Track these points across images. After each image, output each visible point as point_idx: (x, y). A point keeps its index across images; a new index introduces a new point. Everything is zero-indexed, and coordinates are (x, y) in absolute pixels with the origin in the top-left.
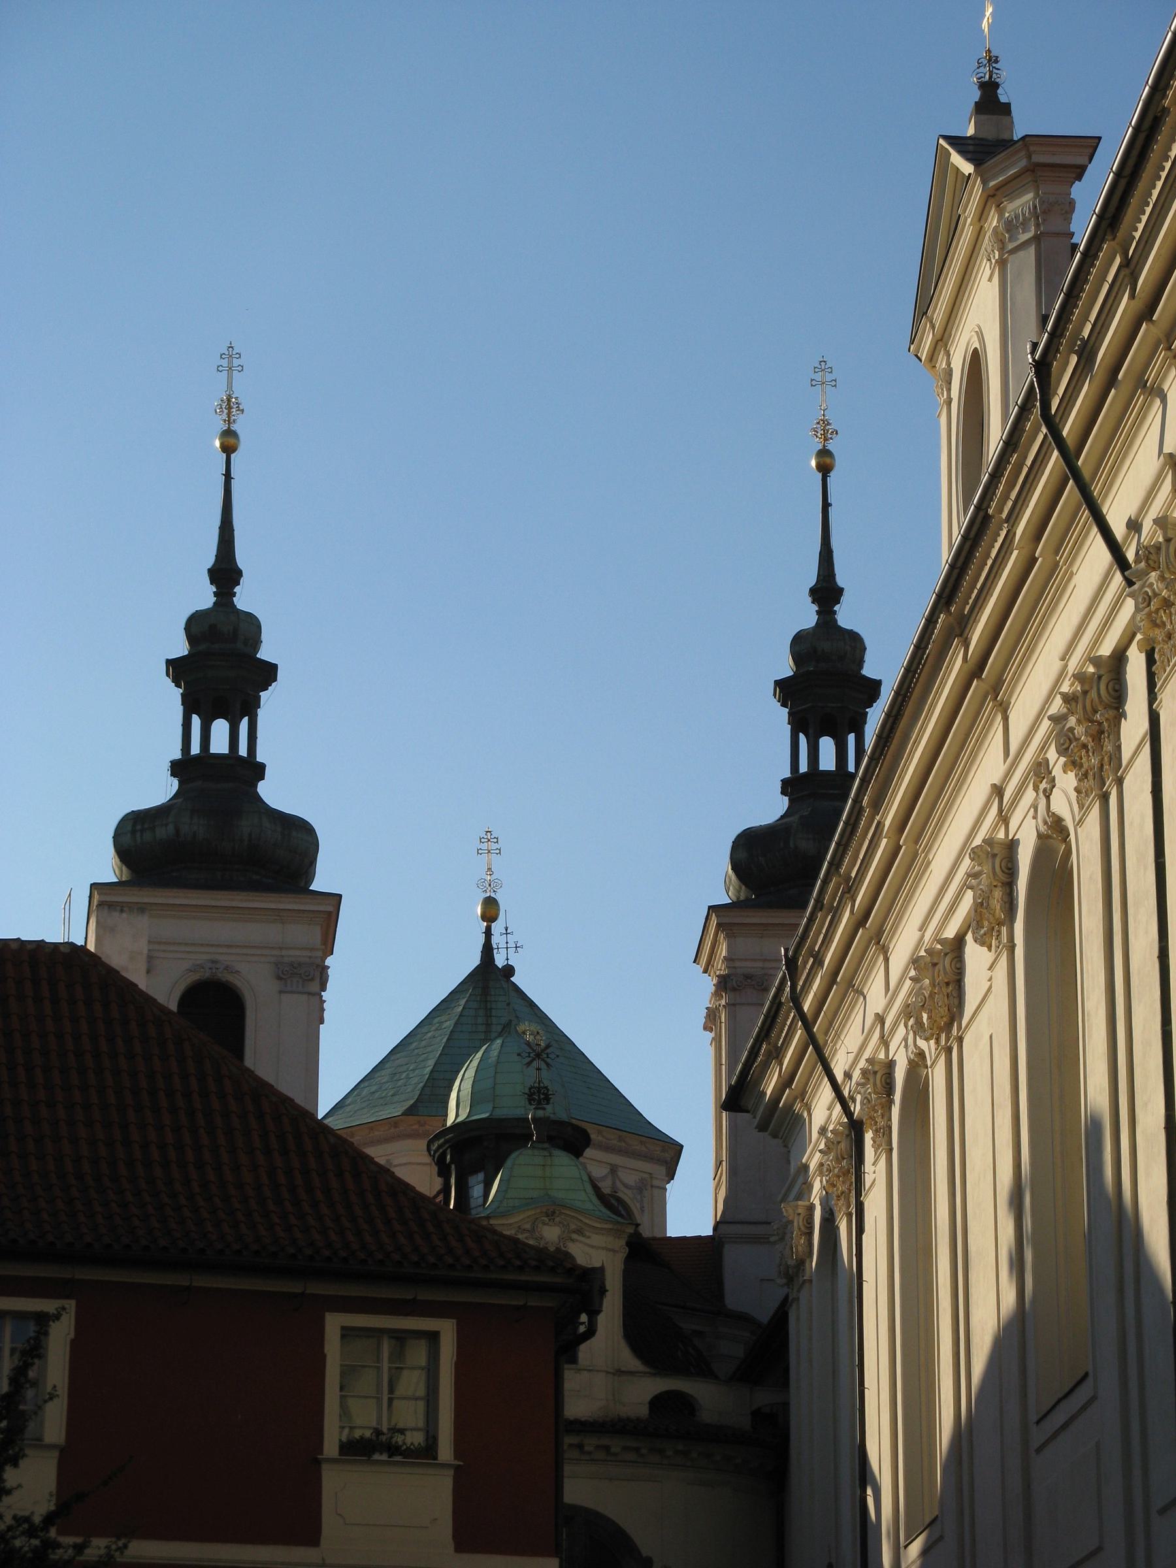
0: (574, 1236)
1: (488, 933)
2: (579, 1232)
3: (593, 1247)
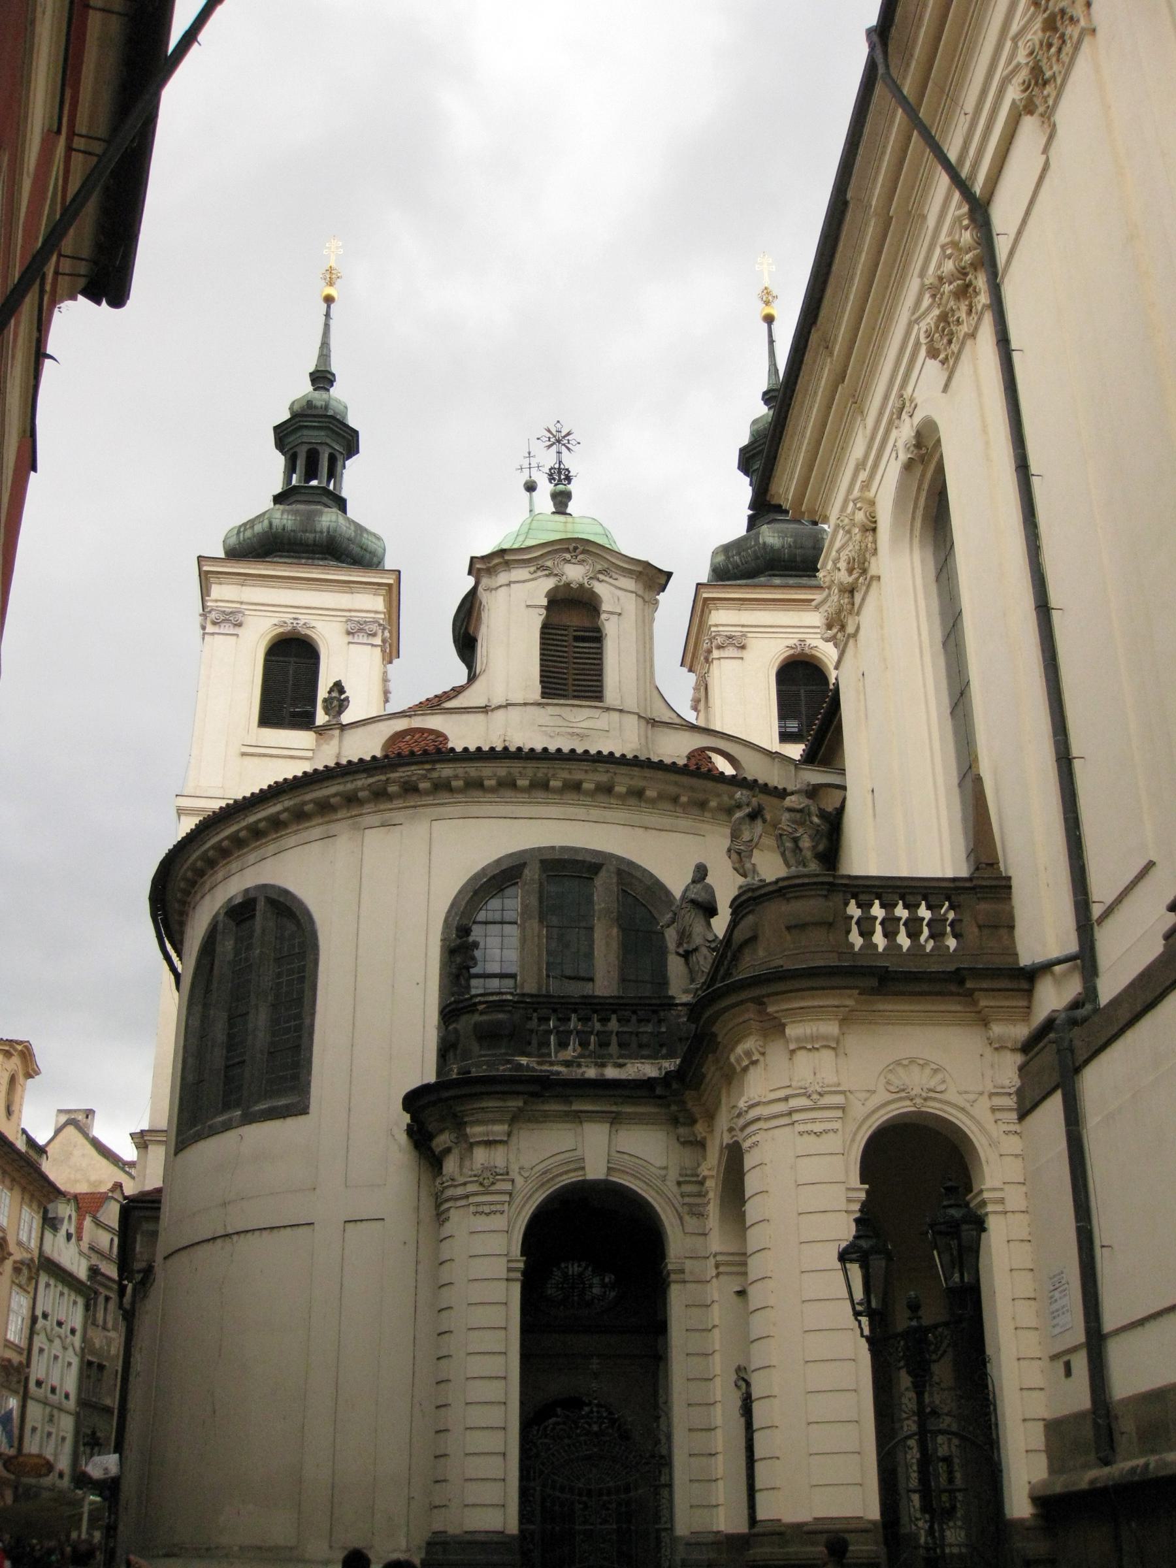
0: (601, 577)
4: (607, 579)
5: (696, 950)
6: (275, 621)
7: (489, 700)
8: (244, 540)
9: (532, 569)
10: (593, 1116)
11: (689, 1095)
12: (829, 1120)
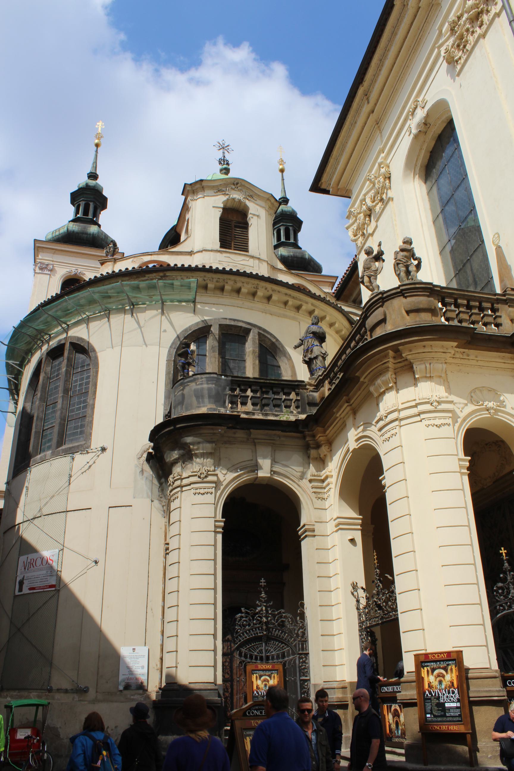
0: (249, 199)
4: (252, 199)
5: (316, 358)
6: (68, 270)
8: (55, 236)
9: (215, 191)
11: (320, 429)
12: (445, 418)
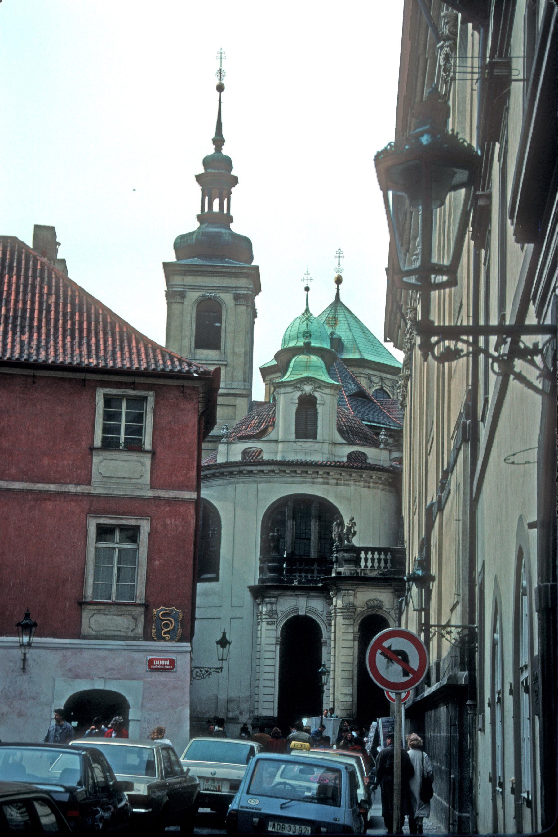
0: (317, 389)
1: (338, 289)
2: (319, 387)
3: (325, 394)
7: (278, 437)
9: (293, 388)
10: (302, 596)
